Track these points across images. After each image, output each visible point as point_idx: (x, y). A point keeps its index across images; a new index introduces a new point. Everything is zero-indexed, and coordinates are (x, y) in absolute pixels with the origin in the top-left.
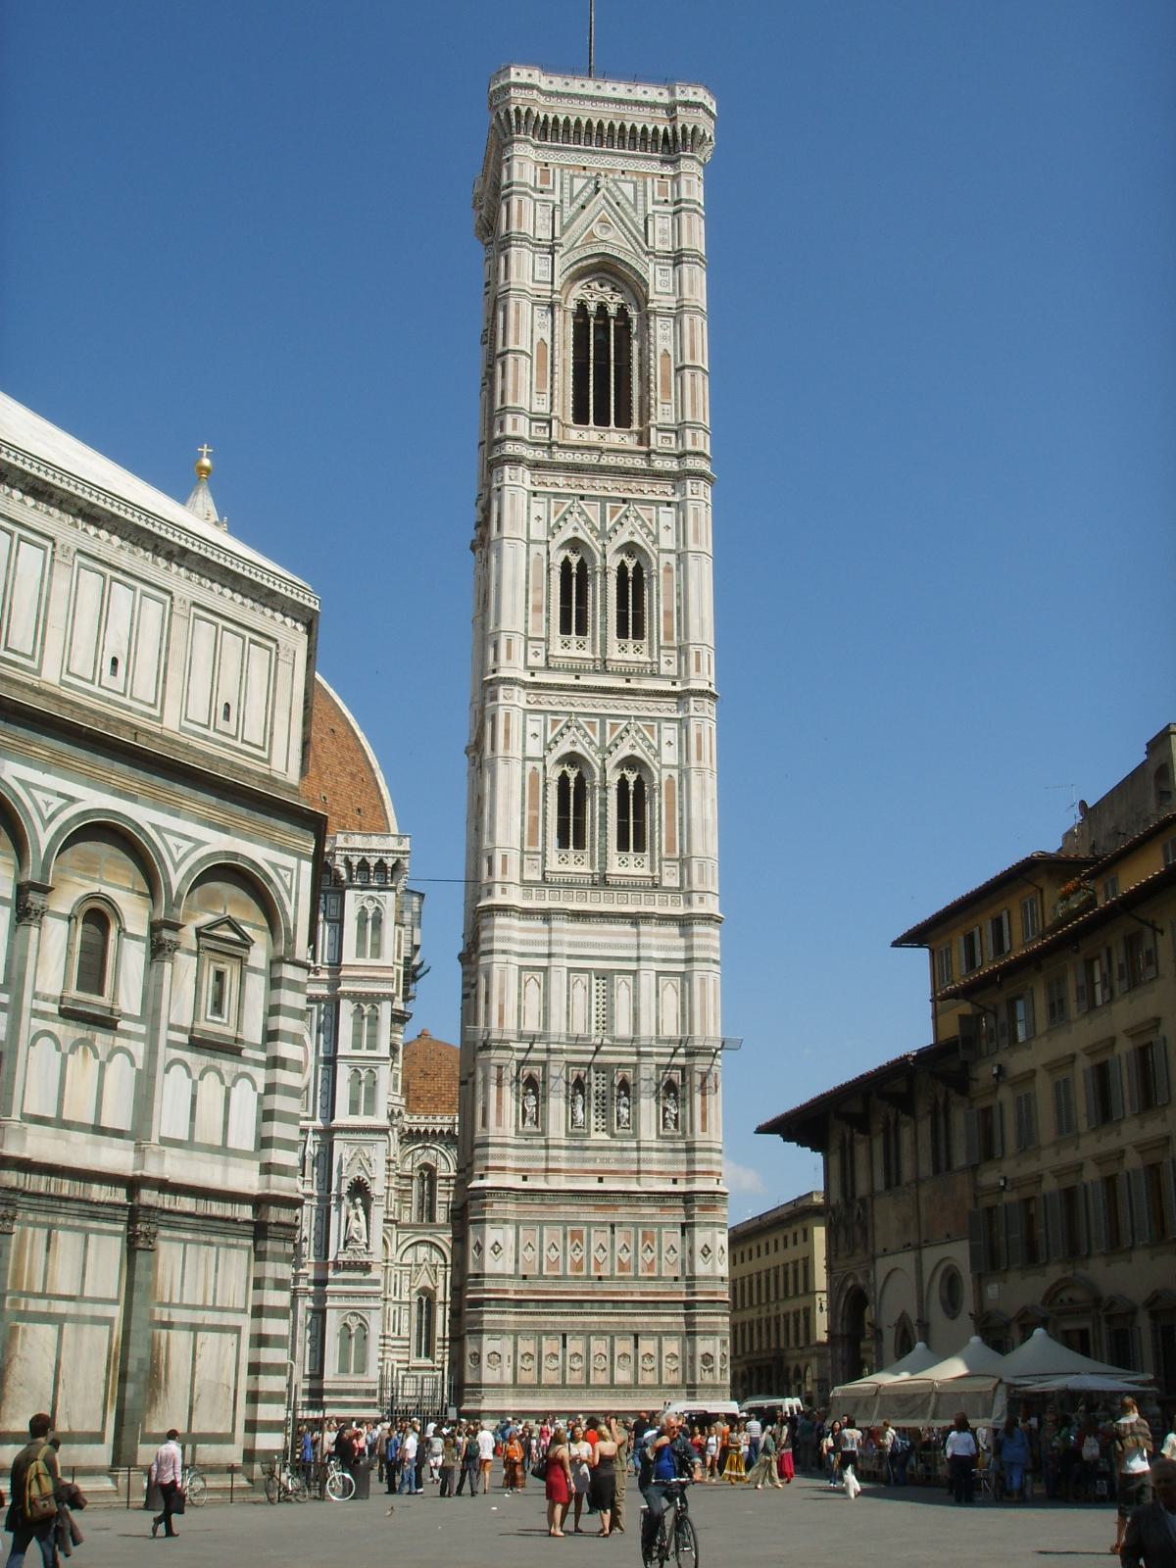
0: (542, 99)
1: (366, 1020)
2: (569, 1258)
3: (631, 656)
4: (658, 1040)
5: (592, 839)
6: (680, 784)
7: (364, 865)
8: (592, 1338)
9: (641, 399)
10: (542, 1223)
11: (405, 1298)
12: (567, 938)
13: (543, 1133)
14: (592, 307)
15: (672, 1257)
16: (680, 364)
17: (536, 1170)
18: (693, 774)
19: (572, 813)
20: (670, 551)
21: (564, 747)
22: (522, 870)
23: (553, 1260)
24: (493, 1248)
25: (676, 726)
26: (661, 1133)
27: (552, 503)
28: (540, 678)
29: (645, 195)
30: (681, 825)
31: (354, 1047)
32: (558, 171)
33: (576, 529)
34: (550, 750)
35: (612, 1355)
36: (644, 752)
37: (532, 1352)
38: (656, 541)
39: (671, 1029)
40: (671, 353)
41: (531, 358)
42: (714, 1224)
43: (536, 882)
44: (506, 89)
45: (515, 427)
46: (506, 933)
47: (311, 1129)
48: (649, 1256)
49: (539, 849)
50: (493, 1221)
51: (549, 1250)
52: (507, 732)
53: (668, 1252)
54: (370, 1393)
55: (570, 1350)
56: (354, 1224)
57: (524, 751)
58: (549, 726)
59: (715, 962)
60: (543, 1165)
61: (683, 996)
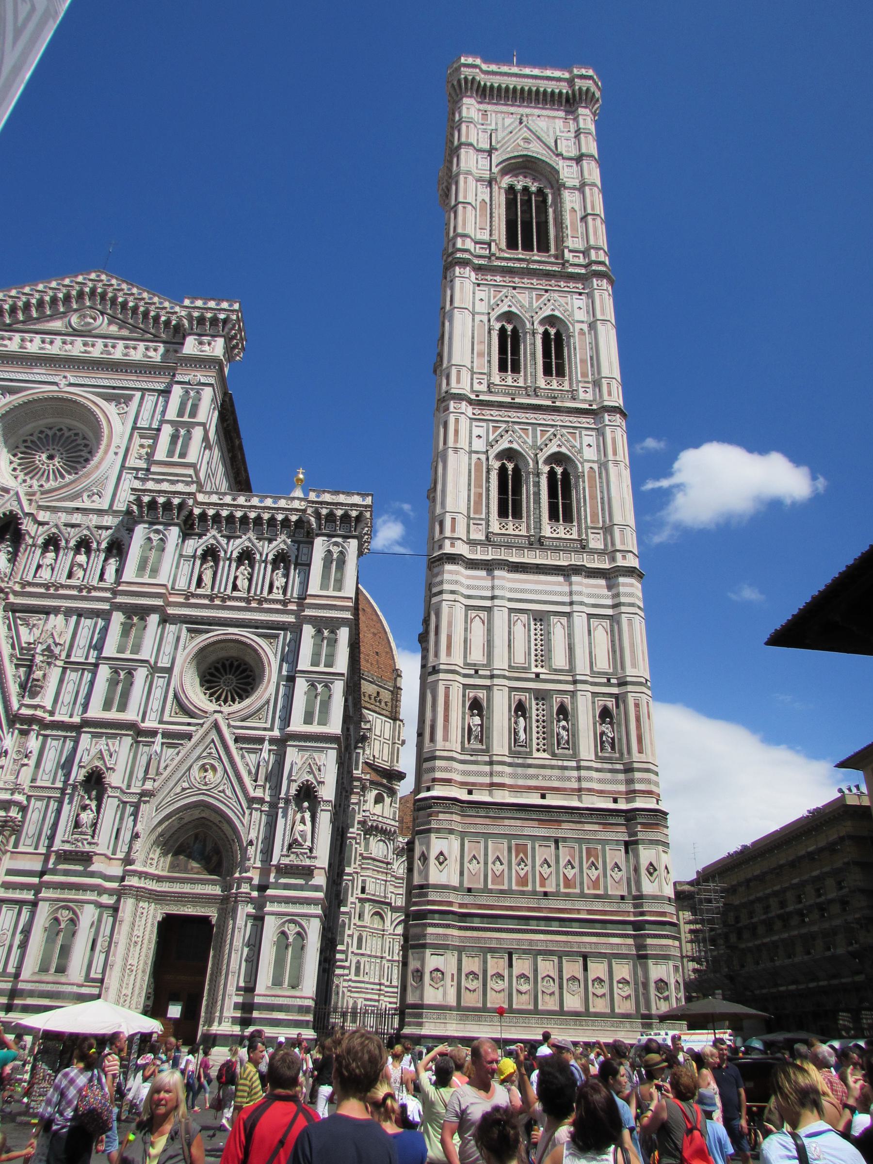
0: (483, 76)
1: (325, 641)
5: (528, 512)
6: (600, 474)
7: (331, 516)
8: (540, 958)
9: (557, 237)
10: (487, 836)
11: (396, 958)
13: (487, 751)
15: (617, 875)
17: (481, 785)
18: (611, 465)
19: (510, 493)
20: (582, 322)
21: (504, 445)
22: (468, 532)
23: (498, 873)
24: (437, 858)
25: (594, 433)
26: (600, 754)
27: (492, 292)
30: (602, 503)
31: (312, 665)
33: (510, 306)
34: (492, 446)
35: (561, 978)
36: (569, 450)
37: (476, 970)
39: (603, 664)
40: (577, 208)
41: (475, 209)
42: (657, 842)
44: (460, 67)
46: (454, 577)
47: (267, 738)
48: (594, 874)
49: (483, 516)
50: (438, 830)
51: (494, 863)
52: (456, 432)
53: (612, 870)
54: (302, 1009)
55: (516, 971)
56: (300, 827)
57: (470, 446)
59: (639, 607)
60: (487, 780)
61: (613, 635)
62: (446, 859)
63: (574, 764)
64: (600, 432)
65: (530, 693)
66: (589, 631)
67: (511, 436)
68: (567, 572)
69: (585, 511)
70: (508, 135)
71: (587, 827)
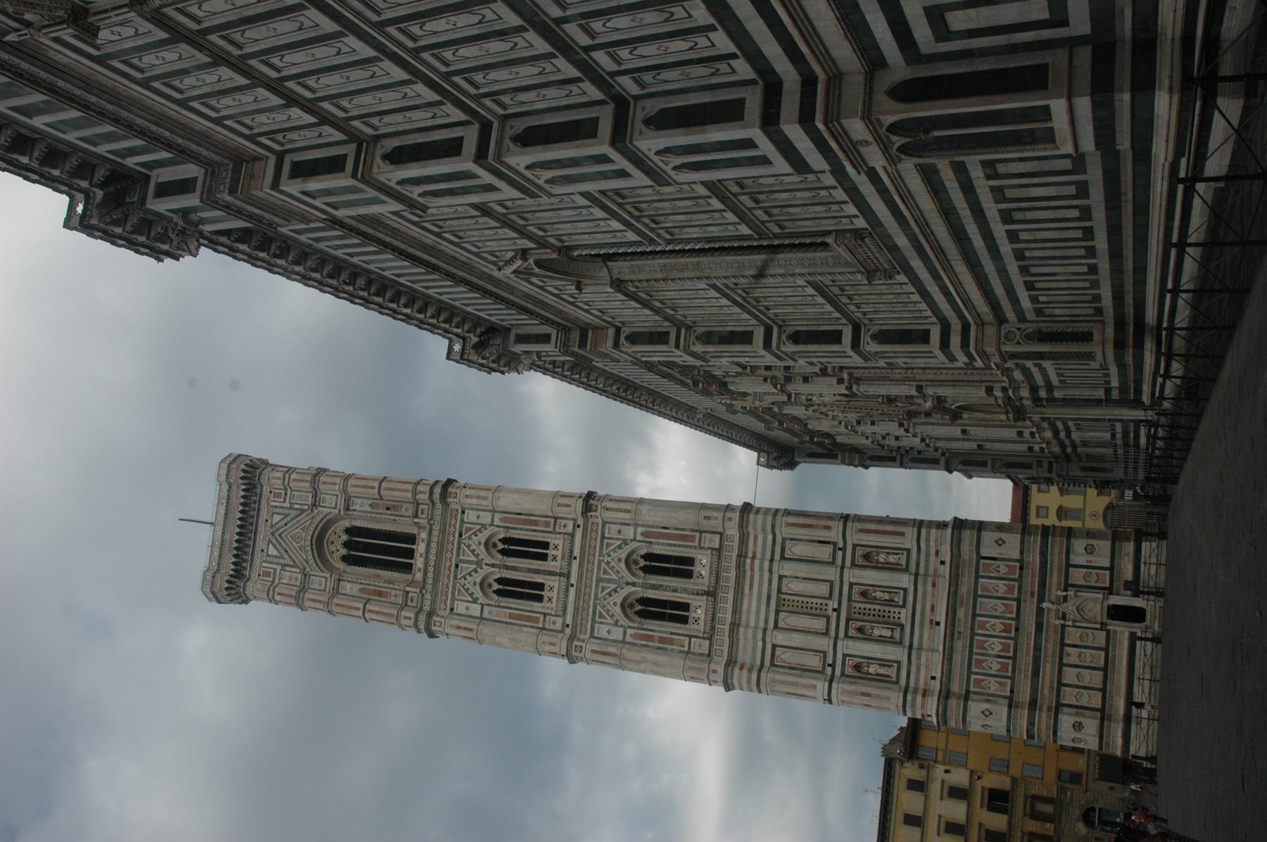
3: (559, 553)
4: (833, 563)
6: (648, 526)
12: (752, 624)
13: (899, 663)
14: (344, 551)
16: (377, 497)
28: (569, 620)
32: (265, 565)
38: (484, 526)
39: (824, 552)
40: (370, 502)
41: (369, 600)
43: (711, 645)
45: (410, 618)
58: (604, 621)
70: (290, 557)
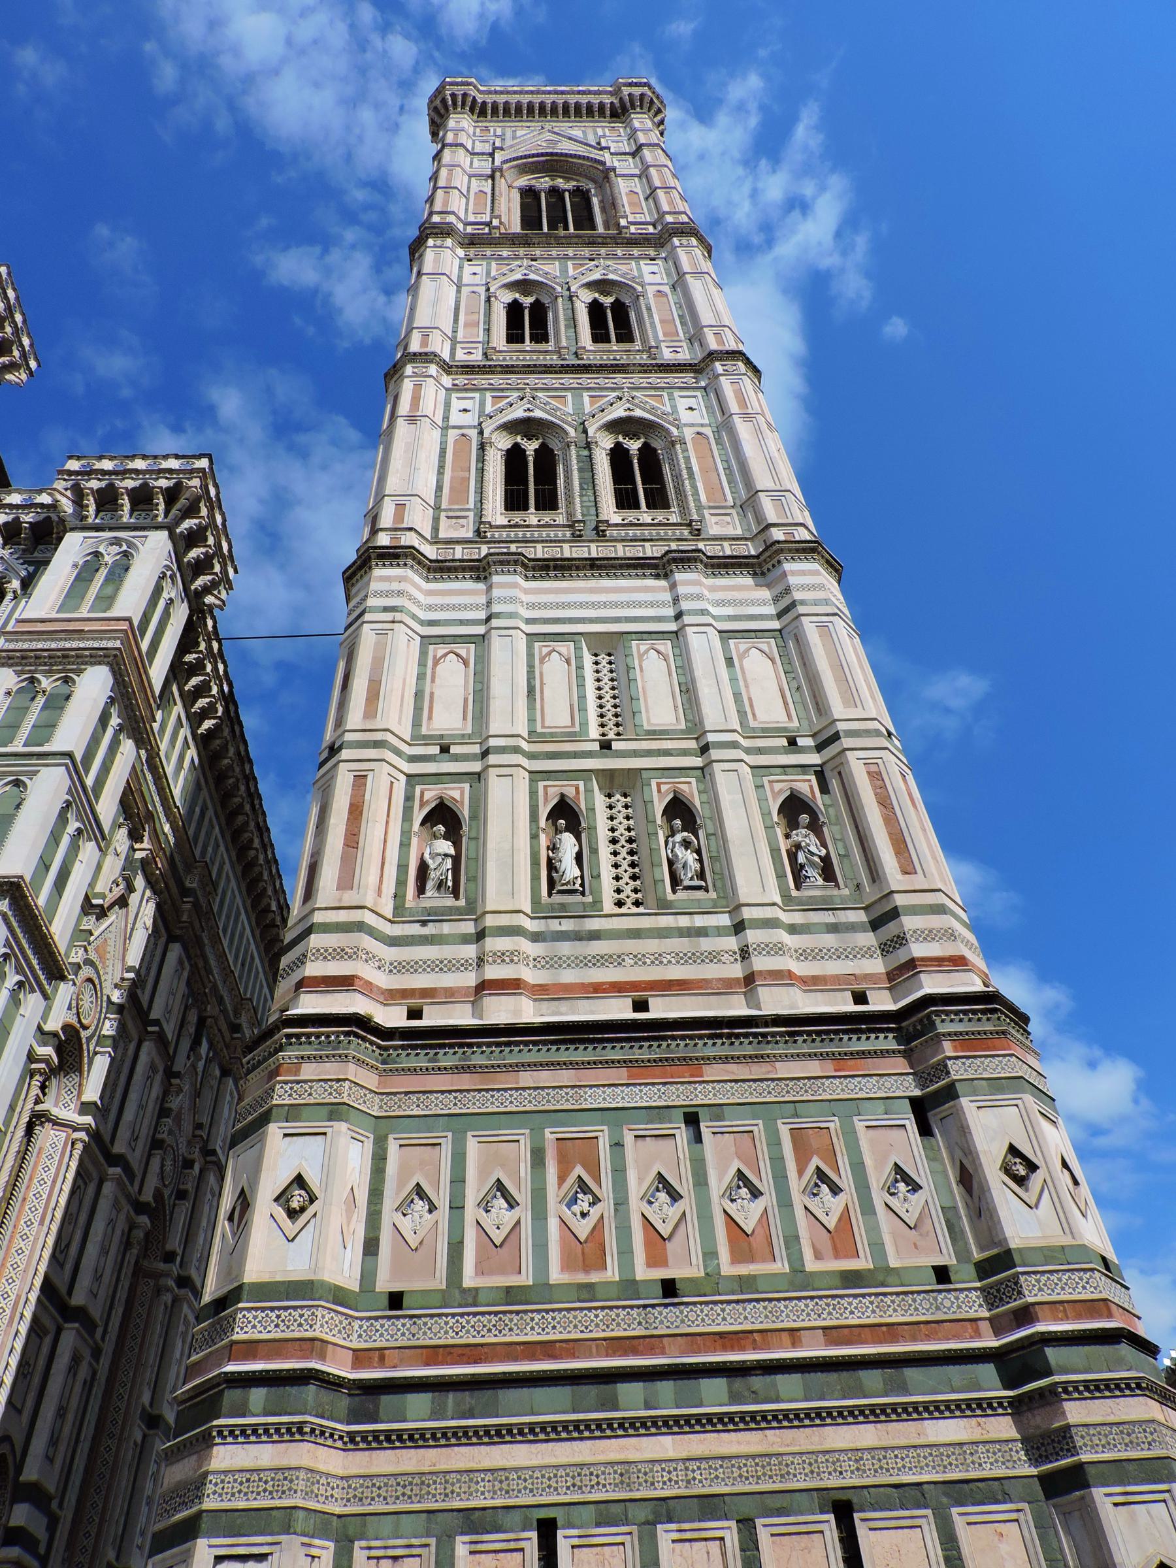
2: (553, 1224)
8: (665, 1535)
18: (737, 421)
19: (531, 479)
22: (436, 529)
25: (698, 394)
26: (794, 893)
29: (596, 133)
42: (1015, 1083)
46: (395, 586)
48: (830, 1207)
49: (471, 506)
62: (312, 1199)
63: (724, 920)
64: (713, 391)
65: (587, 781)
66: (729, 661)
67: (530, 402)
68: (661, 567)
69: (694, 487)
71: (785, 1069)
